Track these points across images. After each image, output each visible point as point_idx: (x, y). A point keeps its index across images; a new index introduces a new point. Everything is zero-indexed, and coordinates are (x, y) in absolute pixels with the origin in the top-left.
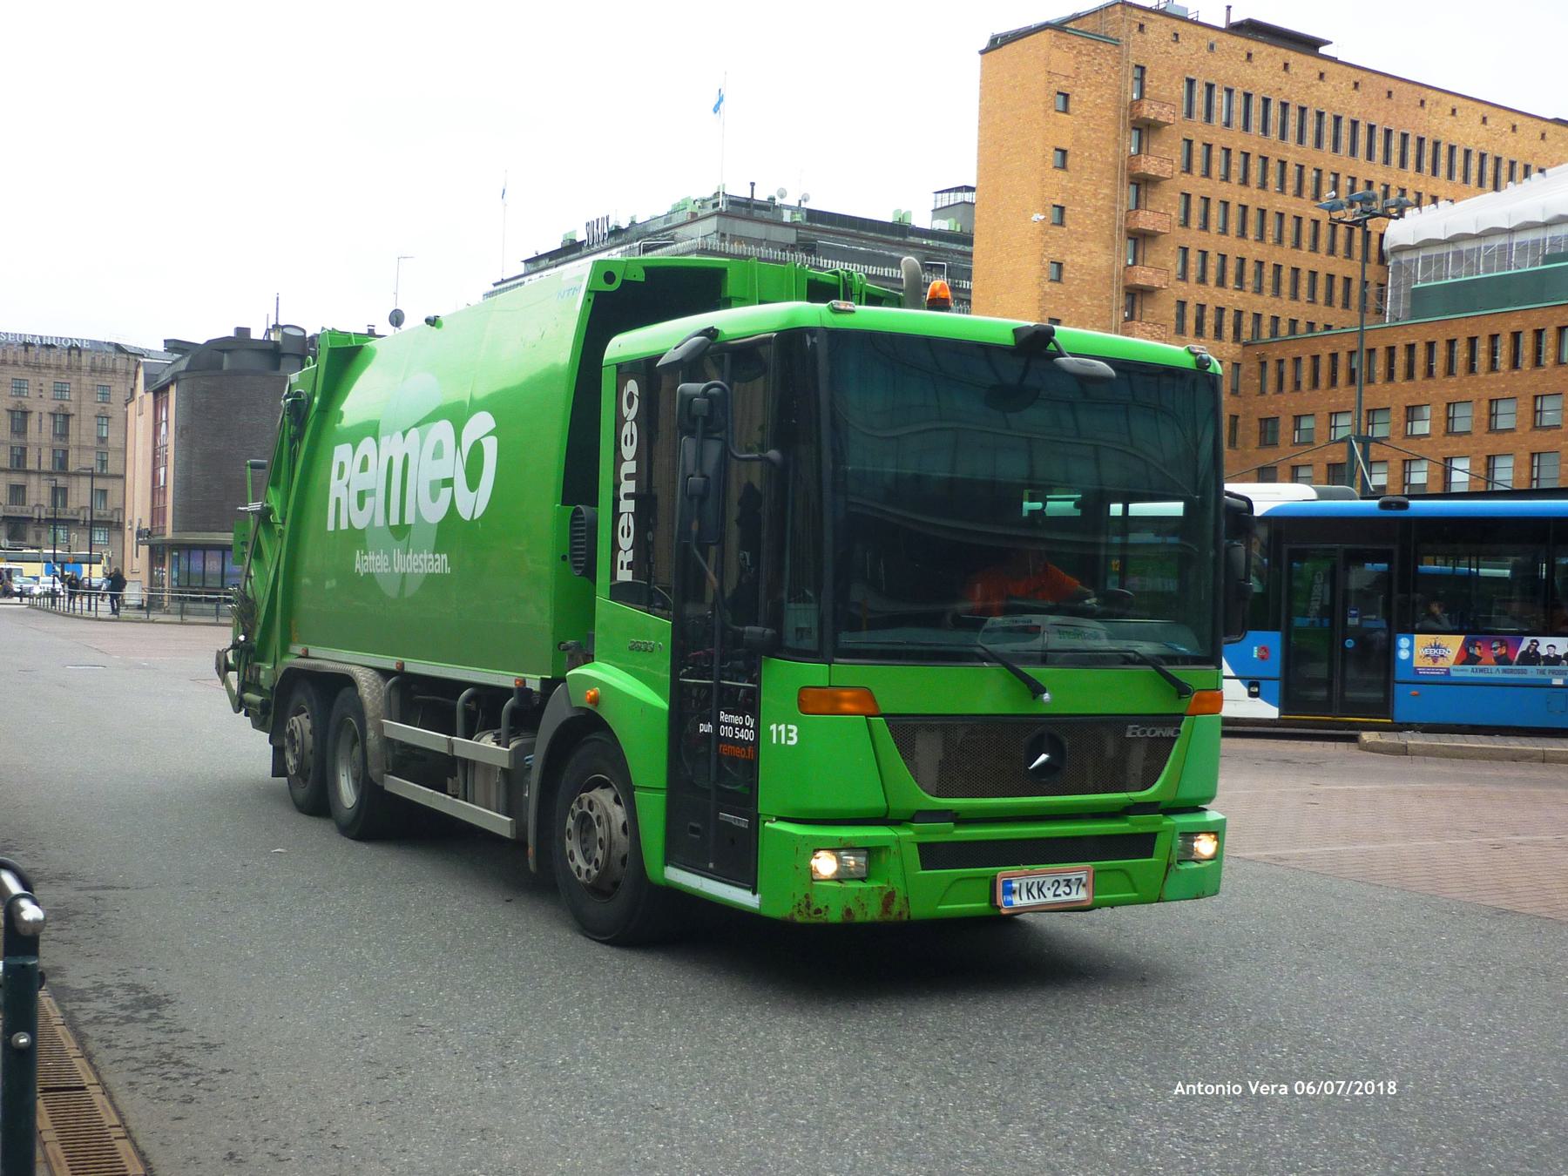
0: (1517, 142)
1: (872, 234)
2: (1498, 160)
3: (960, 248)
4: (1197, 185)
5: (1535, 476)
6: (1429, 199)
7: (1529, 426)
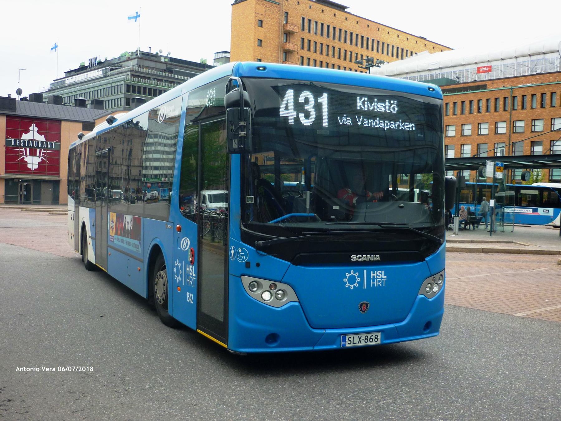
2: (402, 49)
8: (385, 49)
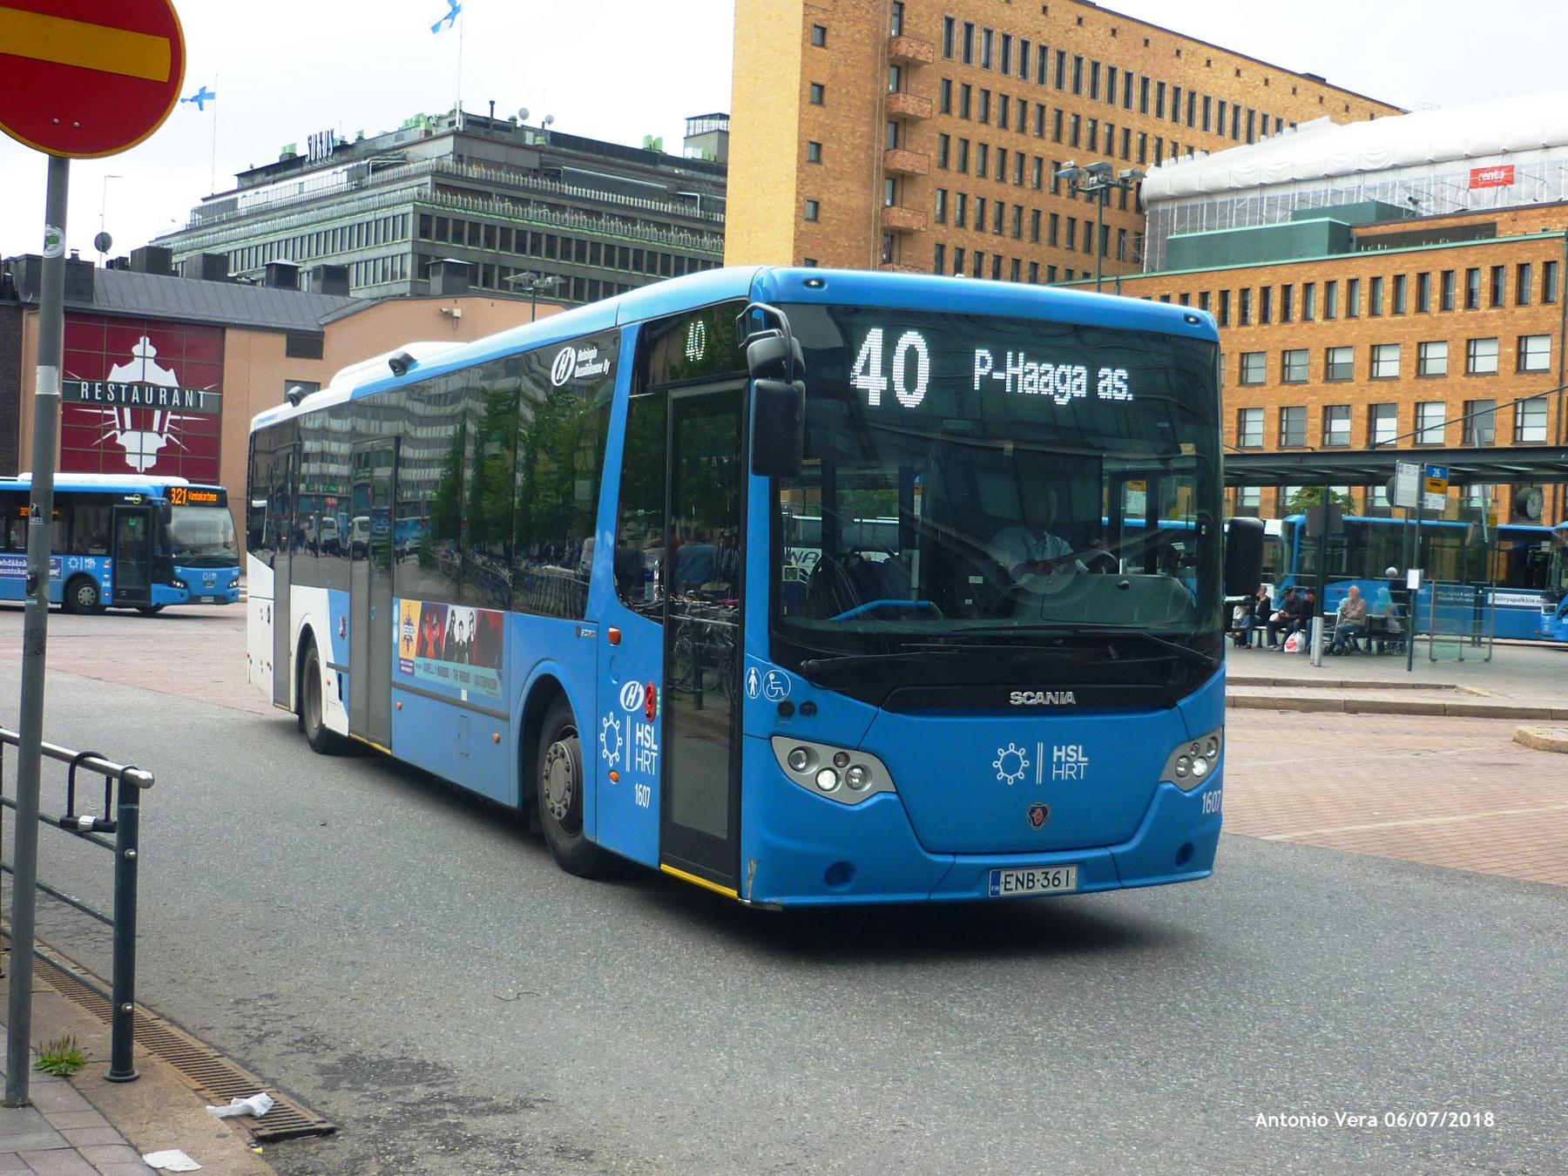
0: (1270, 96)
1: (619, 161)
2: (1251, 113)
3: (714, 178)
4: (956, 126)
5: (1284, 430)
6: (1186, 150)
7: (1278, 381)
8: (1199, 112)
